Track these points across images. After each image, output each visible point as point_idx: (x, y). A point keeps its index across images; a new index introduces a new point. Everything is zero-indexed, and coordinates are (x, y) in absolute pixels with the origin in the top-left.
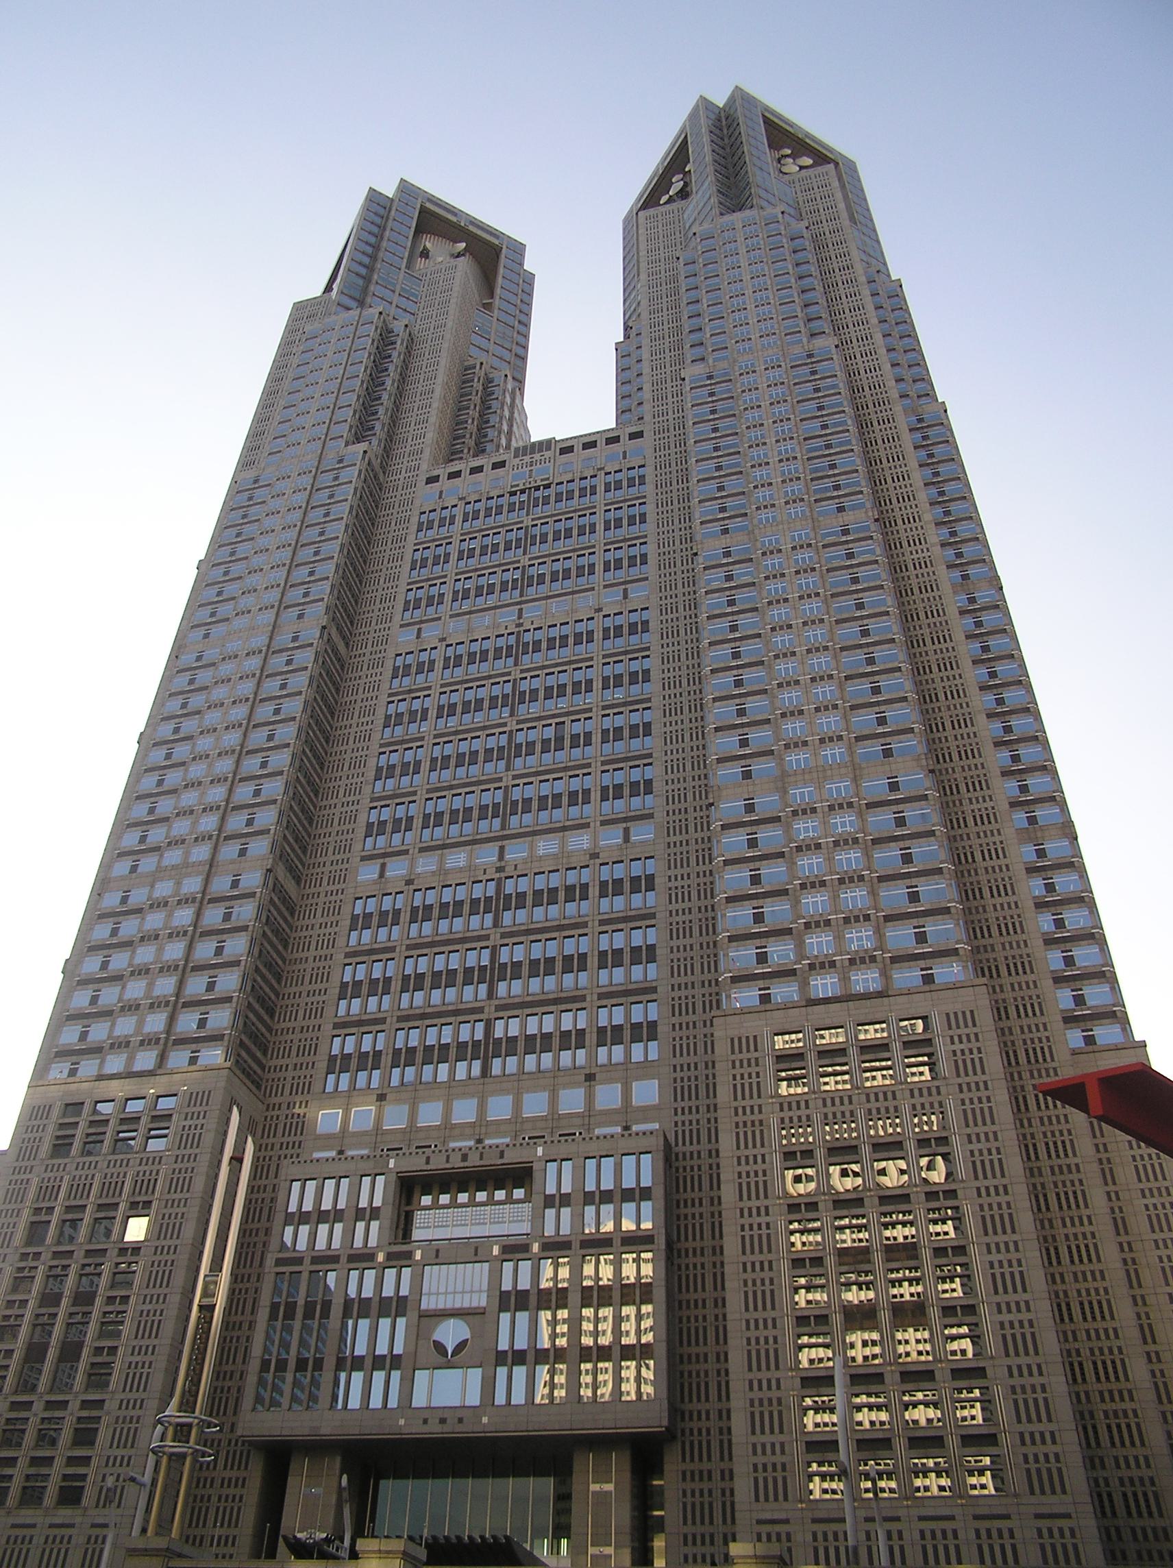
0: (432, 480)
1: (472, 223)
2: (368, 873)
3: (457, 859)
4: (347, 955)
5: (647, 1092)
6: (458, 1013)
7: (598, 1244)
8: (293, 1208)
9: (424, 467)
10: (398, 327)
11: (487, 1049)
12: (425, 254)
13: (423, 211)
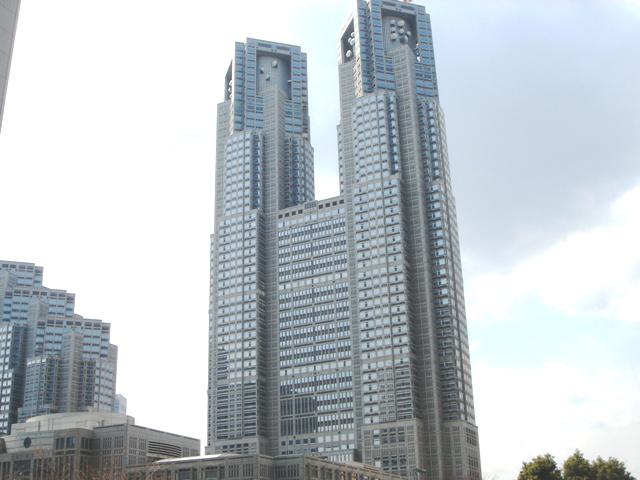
0: (280, 216)
1: (279, 48)
2: (282, 373)
3: (304, 370)
5: (352, 436)
10: (259, 133)
12: (262, 72)
13: (258, 51)
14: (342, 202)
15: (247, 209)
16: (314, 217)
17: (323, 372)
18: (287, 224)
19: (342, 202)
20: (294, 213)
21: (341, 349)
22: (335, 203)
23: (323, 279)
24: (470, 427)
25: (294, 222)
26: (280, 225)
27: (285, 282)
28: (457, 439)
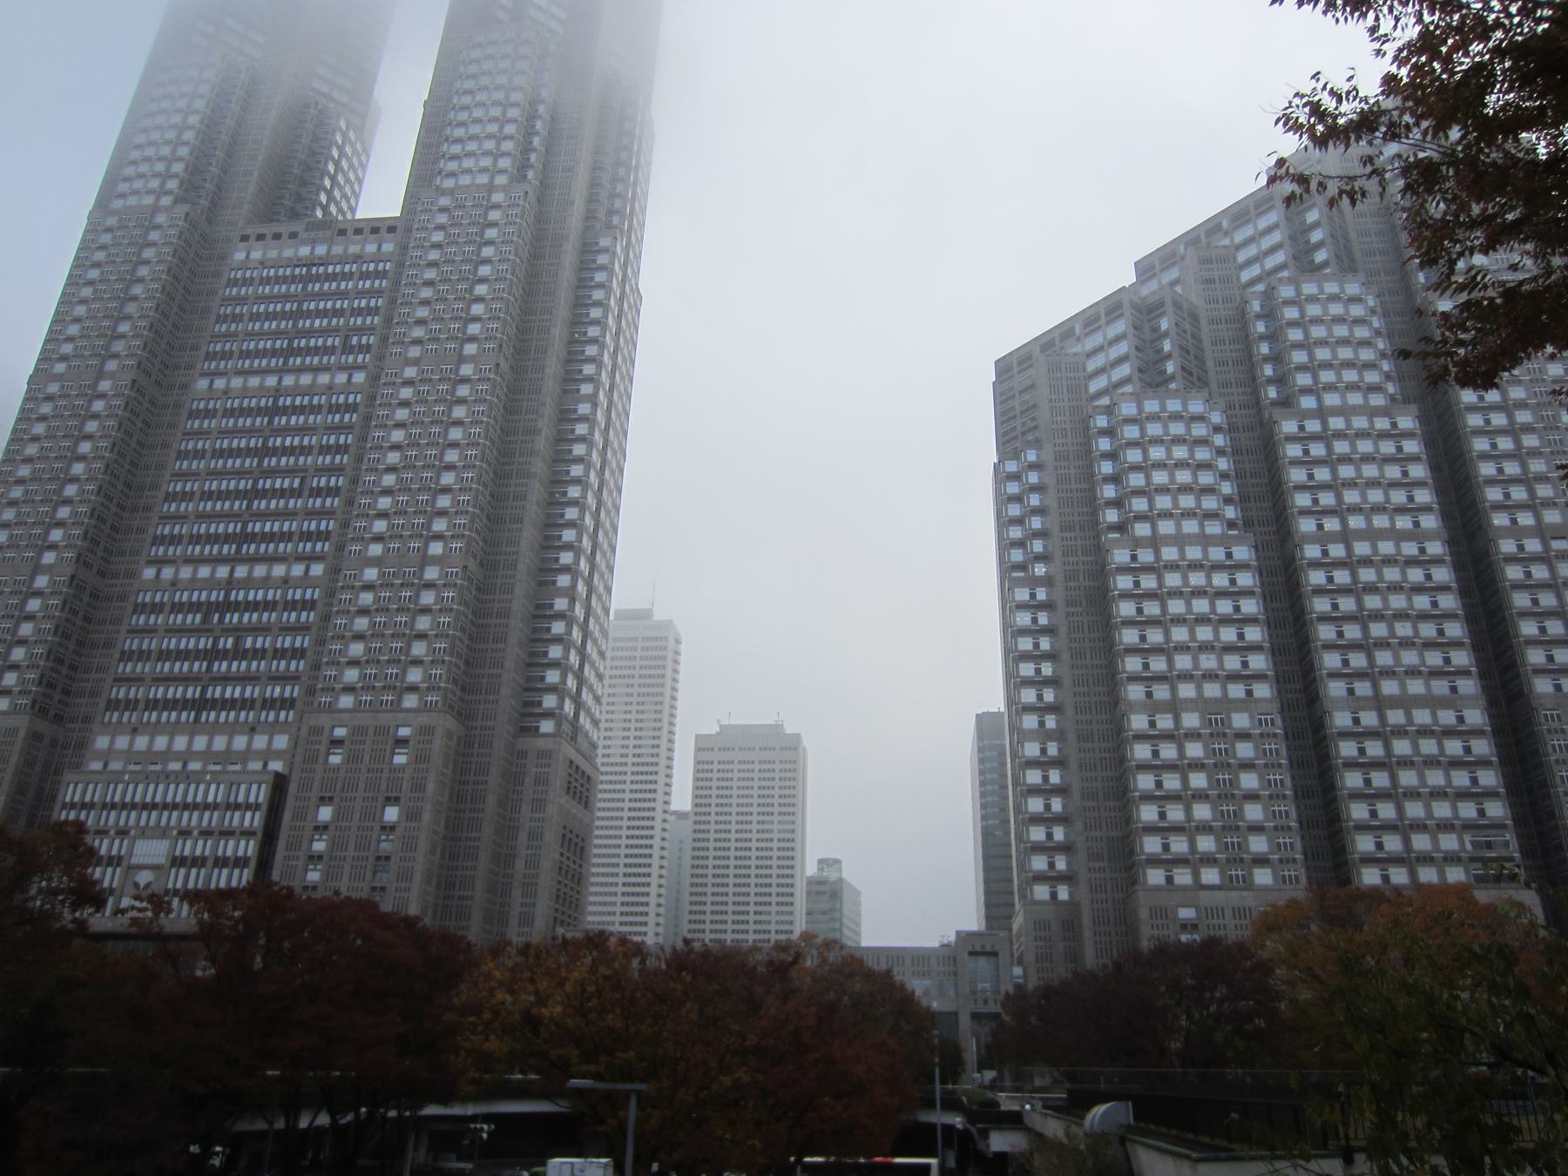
0: (245, 238)
2: (149, 573)
4: (129, 632)
6: (186, 680)
7: (228, 833)
8: (68, 799)
9: (241, 223)
11: (202, 704)
14: (392, 229)
15: (166, 201)
16: (321, 250)
17: (248, 584)
18: (256, 255)
19: (392, 229)
20: (277, 236)
21: (307, 536)
22: (375, 230)
23: (306, 379)
24: (584, 765)
25: (273, 254)
26: (240, 256)
27: (214, 374)
28: (542, 781)
